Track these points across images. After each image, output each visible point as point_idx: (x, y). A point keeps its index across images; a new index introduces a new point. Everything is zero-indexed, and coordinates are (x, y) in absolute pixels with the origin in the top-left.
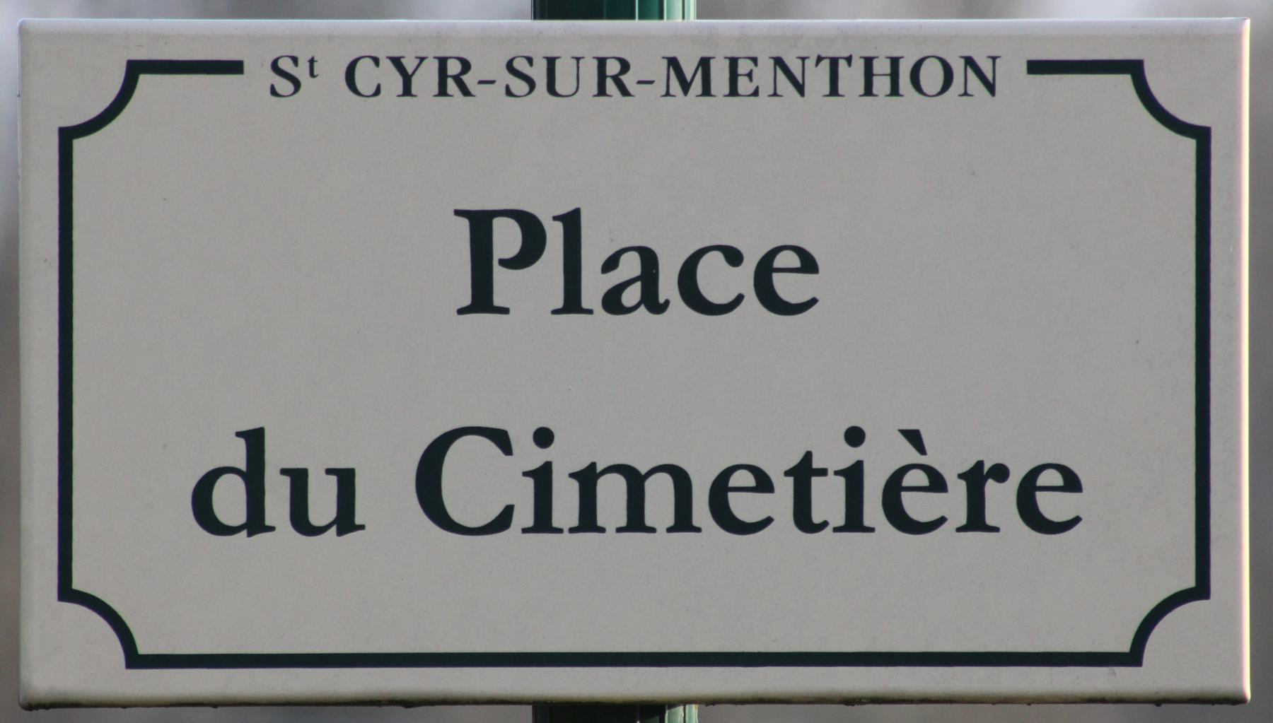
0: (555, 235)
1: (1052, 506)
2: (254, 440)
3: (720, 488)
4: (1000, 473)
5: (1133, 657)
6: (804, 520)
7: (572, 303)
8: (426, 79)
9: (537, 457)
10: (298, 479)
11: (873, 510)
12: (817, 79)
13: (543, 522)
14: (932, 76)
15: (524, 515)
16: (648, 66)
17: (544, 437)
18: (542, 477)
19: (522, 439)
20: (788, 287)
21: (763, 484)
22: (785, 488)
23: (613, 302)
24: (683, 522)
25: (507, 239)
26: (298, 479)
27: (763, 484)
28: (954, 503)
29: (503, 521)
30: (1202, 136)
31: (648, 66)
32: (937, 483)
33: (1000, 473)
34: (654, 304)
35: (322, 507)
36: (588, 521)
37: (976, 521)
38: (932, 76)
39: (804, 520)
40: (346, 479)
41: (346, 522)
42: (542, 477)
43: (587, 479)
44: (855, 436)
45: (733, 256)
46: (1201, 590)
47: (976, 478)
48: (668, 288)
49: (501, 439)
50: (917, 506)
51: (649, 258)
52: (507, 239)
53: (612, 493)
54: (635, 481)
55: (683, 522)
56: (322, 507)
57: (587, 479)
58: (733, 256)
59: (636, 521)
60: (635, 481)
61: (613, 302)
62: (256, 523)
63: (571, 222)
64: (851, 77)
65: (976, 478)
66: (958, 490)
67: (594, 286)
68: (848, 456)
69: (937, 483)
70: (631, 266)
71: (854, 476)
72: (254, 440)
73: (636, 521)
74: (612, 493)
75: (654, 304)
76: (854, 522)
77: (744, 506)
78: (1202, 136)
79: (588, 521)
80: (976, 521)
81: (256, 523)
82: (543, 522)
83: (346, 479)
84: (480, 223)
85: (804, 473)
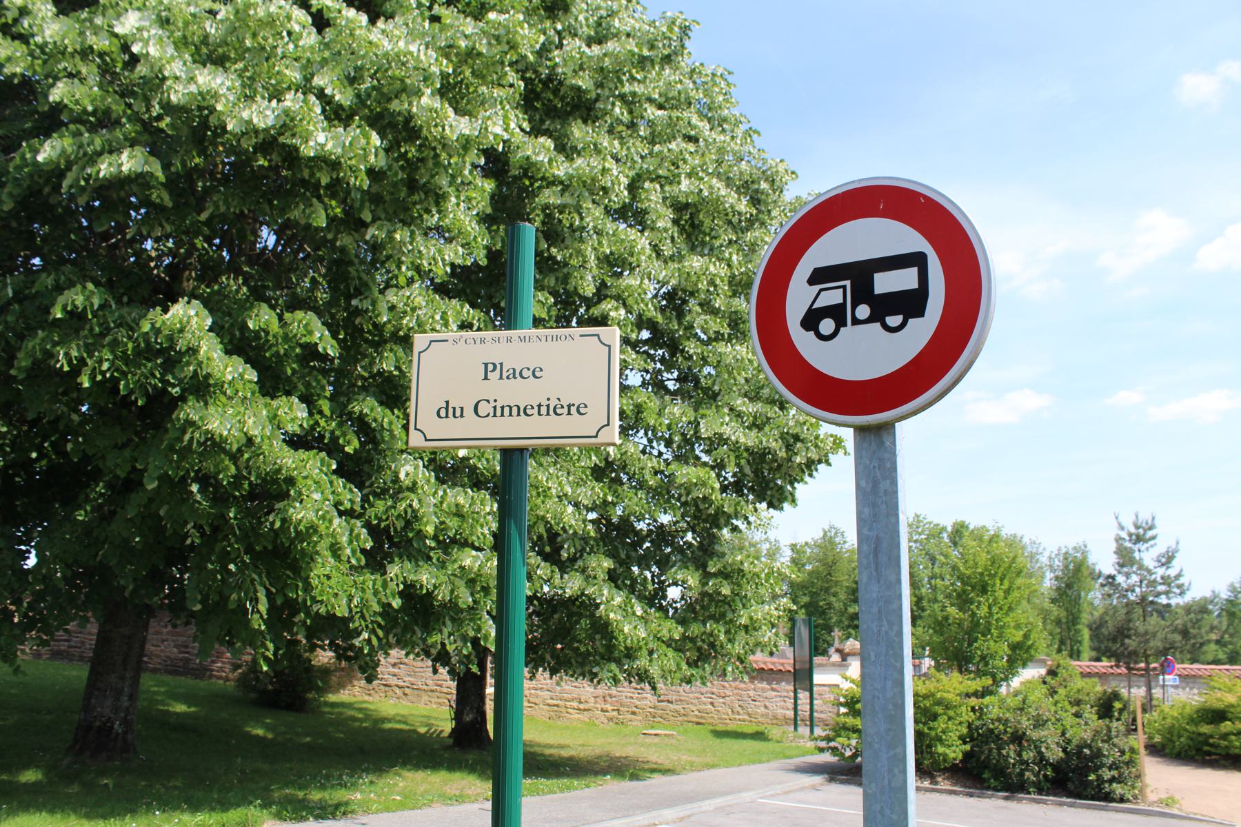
0: (499, 366)
1: (582, 410)
2: (447, 402)
3: (525, 409)
4: (573, 405)
5: (596, 437)
6: (539, 414)
7: (501, 378)
8: (478, 341)
9: (494, 404)
10: (454, 409)
11: (551, 412)
12: (544, 339)
13: (495, 415)
14: (563, 338)
15: (492, 414)
16: (515, 338)
17: (495, 401)
18: (495, 408)
19: (492, 401)
20: (538, 374)
21: (533, 408)
22: (536, 408)
23: (508, 378)
24: (519, 415)
25: (490, 367)
26: (454, 409)
27: (533, 408)
28: (565, 410)
29: (488, 415)
30: (609, 346)
31: (515, 338)
32: (562, 407)
33: (573, 405)
34: (515, 377)
35: (458, 413)
36: (502, 415)
37: (569, 413)
38: (563, 338)
39: (539, 414)
40: (462, 409)
41: (462, 416)
42: (495, 408)
43: (502, 408)
44: (548, 399)
45: (528, 369)
46: (608, 424)
47: (569, 406)
48: (517, 375)
49: (488, 401)
50: (559, 411)
51: (514, 370)
52: (490, 367)
53: (507, 410)
54: (511, 408)
55: (519, 415)
56: (458, 413)
57: (502, 408)
58: (528, 369)
59: (511, 415)
60: (511, 408)
61: (508, 378)
62: (447, 416)
63: (501, 364)
64: (549, 338)
65: (569, 406)
66: (566, 408)
67: (504, 376)
68: (547, 403)
69: (562, 407)
70: (511, 371)
71: (548, 406)
72: (447, 402)
73: (511, 415)
74: (507, 410)
75: (515, 377)
76: (548, 414)
77: (529, 412)
78: (609, 346)
79: (502, 415)
80: (569, 413)
81: (447, 416)
82: (495, 415)
83: (462, 409)
84: (486, 365)
85: (539, 406)
